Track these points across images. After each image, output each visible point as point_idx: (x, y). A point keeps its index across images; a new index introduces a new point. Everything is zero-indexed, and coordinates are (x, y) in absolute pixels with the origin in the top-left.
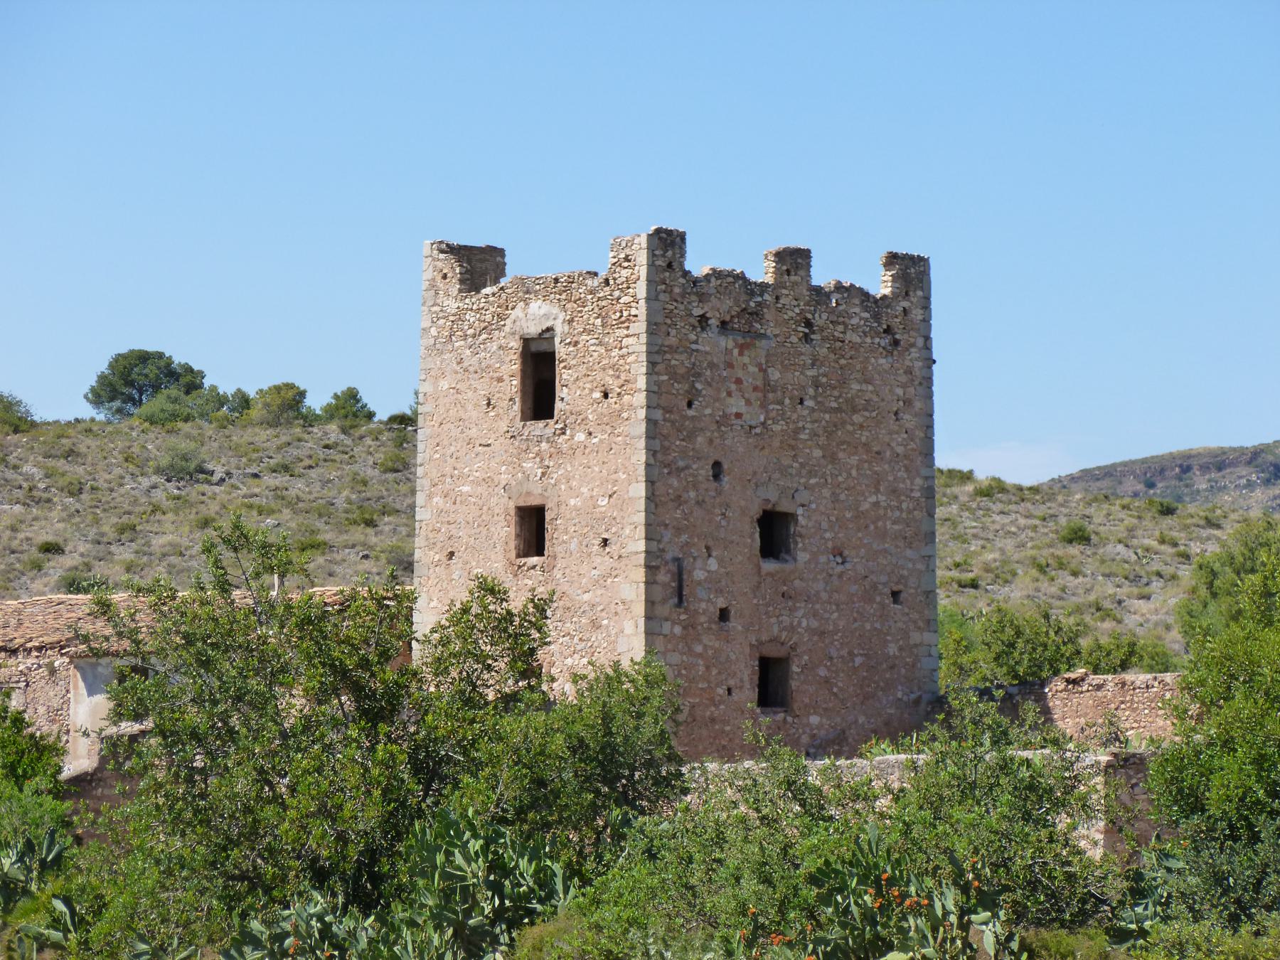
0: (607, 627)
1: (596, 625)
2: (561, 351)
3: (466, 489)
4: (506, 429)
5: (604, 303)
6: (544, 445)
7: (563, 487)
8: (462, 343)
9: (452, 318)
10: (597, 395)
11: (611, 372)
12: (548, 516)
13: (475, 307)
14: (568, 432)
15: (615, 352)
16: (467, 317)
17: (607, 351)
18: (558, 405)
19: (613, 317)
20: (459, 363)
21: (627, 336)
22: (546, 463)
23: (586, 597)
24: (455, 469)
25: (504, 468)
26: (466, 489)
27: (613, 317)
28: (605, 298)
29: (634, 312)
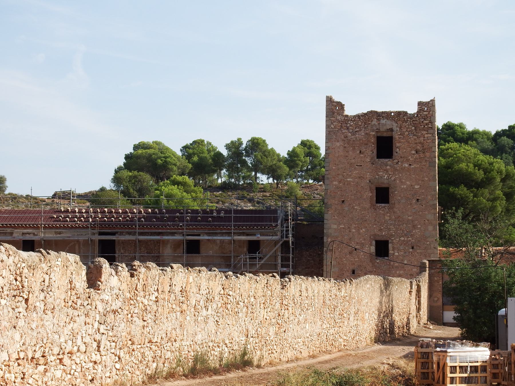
0: (420, 228)
1: (414, 227)
2: (396, 136)
3: (349, 180)
4: (369, 161)
5: (415, 122)
6: (388, 167)
7: (398, 181)
8: (347, 131)
9: (341, 122)
10: (414, 152)
11: (420, 145)
12: (390, 190)
13: (353, 119)
14: (399, 163)
15: (422, 139)
16: (349, 122)
17: (418, 138)
21: (427, 134)
22: (390, 173)
23: (410, 218)
24: (344, 173)
25: (368, 174)
26: (349, 180)
27: (420, 127)
29: (429, 126)
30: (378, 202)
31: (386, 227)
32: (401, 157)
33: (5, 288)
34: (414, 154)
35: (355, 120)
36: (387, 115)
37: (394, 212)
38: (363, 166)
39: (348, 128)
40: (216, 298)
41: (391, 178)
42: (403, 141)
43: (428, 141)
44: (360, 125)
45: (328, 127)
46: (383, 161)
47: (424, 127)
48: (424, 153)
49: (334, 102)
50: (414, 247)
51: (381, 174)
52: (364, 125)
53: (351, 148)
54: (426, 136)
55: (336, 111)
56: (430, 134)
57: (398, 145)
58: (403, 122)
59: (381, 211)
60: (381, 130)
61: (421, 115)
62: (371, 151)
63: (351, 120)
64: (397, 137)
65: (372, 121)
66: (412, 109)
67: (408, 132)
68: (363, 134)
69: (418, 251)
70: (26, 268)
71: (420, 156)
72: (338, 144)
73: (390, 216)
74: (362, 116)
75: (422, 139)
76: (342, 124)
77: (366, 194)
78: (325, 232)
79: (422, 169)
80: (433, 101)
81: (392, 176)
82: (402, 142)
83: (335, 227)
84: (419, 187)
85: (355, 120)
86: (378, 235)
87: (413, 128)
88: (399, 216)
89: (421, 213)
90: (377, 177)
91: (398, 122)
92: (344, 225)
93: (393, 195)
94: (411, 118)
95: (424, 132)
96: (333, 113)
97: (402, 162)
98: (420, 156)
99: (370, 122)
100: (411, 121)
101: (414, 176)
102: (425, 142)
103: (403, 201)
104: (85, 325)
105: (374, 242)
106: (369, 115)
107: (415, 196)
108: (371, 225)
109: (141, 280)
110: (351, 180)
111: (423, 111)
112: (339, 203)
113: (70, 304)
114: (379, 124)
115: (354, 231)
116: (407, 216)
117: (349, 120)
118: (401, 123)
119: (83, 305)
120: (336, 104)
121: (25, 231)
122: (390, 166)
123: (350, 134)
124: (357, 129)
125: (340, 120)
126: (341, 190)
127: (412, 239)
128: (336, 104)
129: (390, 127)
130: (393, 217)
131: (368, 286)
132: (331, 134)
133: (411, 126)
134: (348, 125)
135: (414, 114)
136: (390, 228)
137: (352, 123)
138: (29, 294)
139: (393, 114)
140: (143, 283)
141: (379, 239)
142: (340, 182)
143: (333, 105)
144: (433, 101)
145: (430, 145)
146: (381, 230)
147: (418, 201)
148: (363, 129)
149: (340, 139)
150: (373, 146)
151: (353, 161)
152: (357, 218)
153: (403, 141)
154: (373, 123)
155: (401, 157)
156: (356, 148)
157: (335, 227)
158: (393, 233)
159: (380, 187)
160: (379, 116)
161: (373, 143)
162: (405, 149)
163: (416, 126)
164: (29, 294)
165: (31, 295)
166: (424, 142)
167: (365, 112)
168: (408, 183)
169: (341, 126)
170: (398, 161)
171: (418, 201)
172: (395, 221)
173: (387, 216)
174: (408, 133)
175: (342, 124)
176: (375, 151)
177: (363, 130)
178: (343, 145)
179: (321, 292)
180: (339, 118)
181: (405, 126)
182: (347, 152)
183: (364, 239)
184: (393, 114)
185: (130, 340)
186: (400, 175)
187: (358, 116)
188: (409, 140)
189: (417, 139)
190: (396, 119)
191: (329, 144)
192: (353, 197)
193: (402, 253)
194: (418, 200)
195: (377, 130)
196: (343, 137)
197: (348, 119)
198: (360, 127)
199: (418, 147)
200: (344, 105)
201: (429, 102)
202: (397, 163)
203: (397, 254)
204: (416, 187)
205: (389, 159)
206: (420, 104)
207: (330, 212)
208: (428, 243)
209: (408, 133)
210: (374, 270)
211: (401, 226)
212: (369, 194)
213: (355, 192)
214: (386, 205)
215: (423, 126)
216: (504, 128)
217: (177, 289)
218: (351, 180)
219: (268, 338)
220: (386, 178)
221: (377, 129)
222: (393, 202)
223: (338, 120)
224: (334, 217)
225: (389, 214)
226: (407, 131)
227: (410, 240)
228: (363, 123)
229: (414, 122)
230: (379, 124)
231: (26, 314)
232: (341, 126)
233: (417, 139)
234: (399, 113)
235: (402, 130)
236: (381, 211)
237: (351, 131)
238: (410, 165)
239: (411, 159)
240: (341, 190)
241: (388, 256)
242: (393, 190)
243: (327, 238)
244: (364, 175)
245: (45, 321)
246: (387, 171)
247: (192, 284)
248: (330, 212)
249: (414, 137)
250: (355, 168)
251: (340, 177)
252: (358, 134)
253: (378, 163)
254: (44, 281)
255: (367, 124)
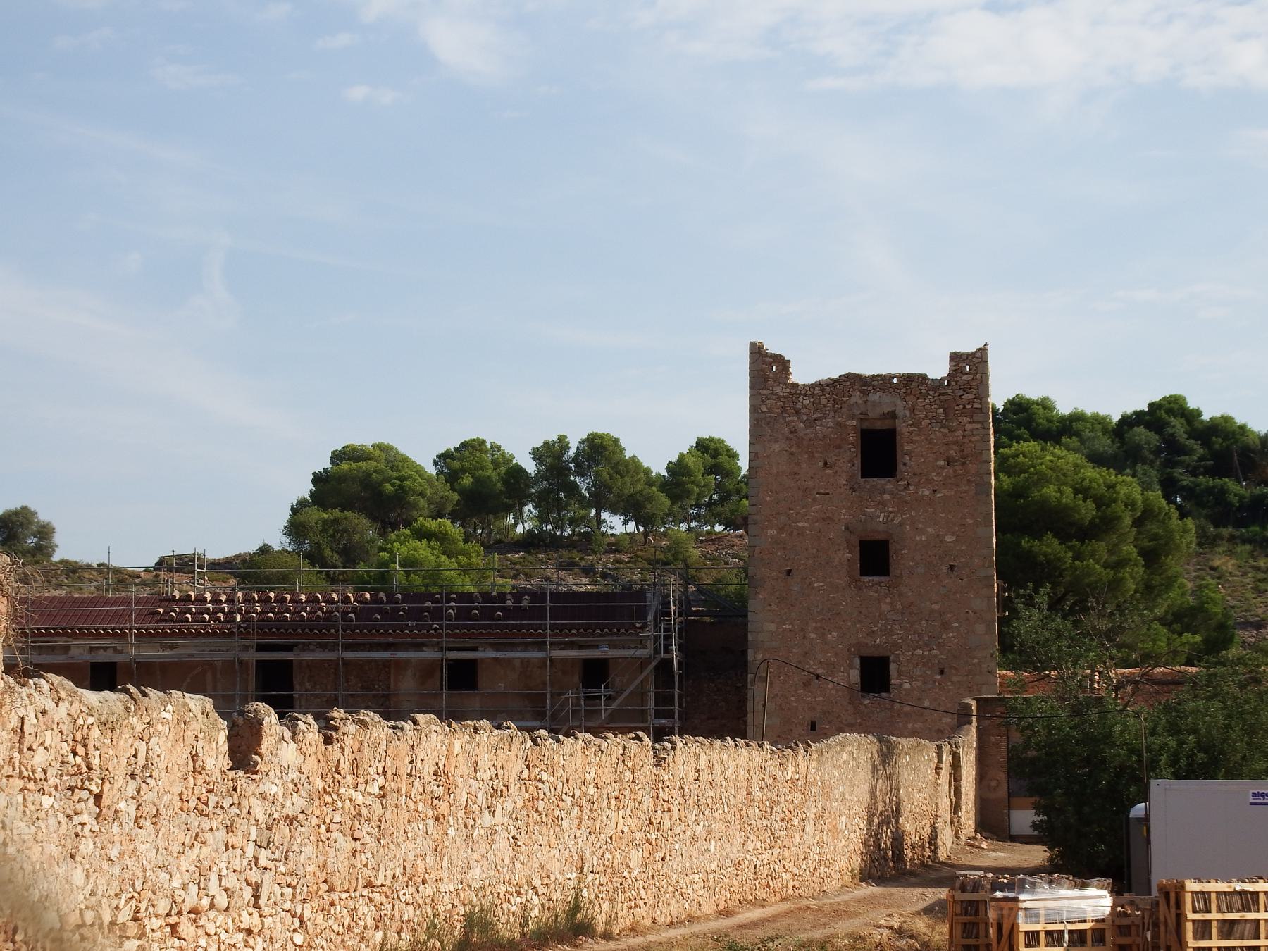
1: (945, 626)
2: (903, 429)
3: (800, 524)
4: (844, 482)
5: (945, 397)
6: (887, 497)
7: (908, 527)
8: (796, 419)
9: (782, 399)
10: (942, 463)
11: (955, 447)
12: (891, 547)
13: (809, 393)
14: (911, 488)
15: (960, 433)
16: (801, 399)
18: (900, 467)
19: (956, 408)
20: (791, 432)
21: (970, 422)
22: (890, 509)
23: (936, 607)
24: (790, 509)
26: (800, 524)
27: (956, 408)
28: (947, 394)
29: (976, 406)
30: (865, 572)
31: (883, 628)
32: (915, 474)
33: (51, 772)
34: (942, 468)
35: (813, 395)
36: (881, 382)
37: (901, 595)
38: (831, 495)
39: (797, 413)
40: (513, 788)
41: (892, 520)
42: (917, 438)
43: (973, 439)
44: (825, 406)
45: (753, 409)
46: (874, 483)
47: (964, 407)
48: (964, 464)
49: (766, 355)
50: (945, 670)
51: (872, 512)
52: (834, 406)
53: (806, 456)
54: (968, 427)
55: (771, 375)
56: (978, 422)
57: (907, 447)
58: (918, 398)
59: (871, 594)
60: (871, 415)
61: (956, 382)
62: (849, 462)
63: (805, 395)
64: (905, 430)
65: (850, 396)
66: (938, 370)
67: (930, 419)
68: (831, 424)
69: (954, 679)
70: (95, 725)
71: (955, 471)
72: (777, 447)
73: (891, 603)
74: (828, 385)
75: (960, 433)
76: (784, 402)
77: (840, 555)
78: (750, 638)
79: (960, 500)
80: (982, 351)
81: (894, 517)
82: (916, 441)
83: (772, 627)
84: (953, 538)
85: (813, 395)
86: (867, 644)
87: (941, 410)
88: (912, 603)
89: (958, 596)
90: (862, 518)
91: (907, 398)
92: (791, 624)
93: (897, 557)
94: (935, 389)
95: (965, 420)
96: (766, 379)
97: (917, 485)
98: (955, 471)
99: (845, 399)
100: (936, 394)
101: (943, 515)
102: (966, 440)
103: (920, 570)
104: (227, 849)
105: (857, 662)
106: (844, 383)
107: (947, 559)
108: (849, 624)
109: (347, 751)
110: (806, 524)
111: (961, 372)
112: (781, 575)
113: (192, 804)
114: (865, 402)
115: (813, 635)
116: (928, 603)
117: (800, 395)
118: (914, 399)
119: (222, 808)
120: (771, 360)
121: (96, 643)
122: (891, 493)
123: (802, 425)
124: (818, 415)
125: (781, 394)
126: (784, 548)
127: (941, 654)
128: (771, 360)
129: (889, 409)
130: (899, 606)
131: (845, 757)
132: (761, 426)
133: (936, 406)
134: (799, 406)
135: (943, 379)
136: (891, 630)
137: (808, 402)
138: (102, 784)
139: (895, 381)
140: (352, 757)
141: (867, 652)
142: (781, 530)
143: (764, 362)
144: (982, 351)
145: (977, 448)
146: (871, 634)
147: (952, 570)
148: (832, 414)
149: (780, 437)
150: (852, 450)
151: (810, 483)
152: (820, 607)
153: (917, 438)
154: (853, 400)
155: (915, 474)
156: (816, 455)
157: (772, 627)
158: (900, 641)
159: (869, 539)
160: (865, 384)
161: (852, 444)
162: (922, 456)
163: (946, 406)
164: (102, 784)
165: (107, 786)
166: (964, 440)
167: (835, 376)
168: (929, 530)
169: (784, 408)
170: (909, 484)
171: (952, 570)
172: (903, 613)
173: (886, 603)
174: (928, 421)
175: (784, 402)
176: (858, 462)
177: (830, 416)
178: (787, 449)
179: (742, 772)
180: (778, 389)
181: (924, 406)
182: (798, 464)
183: (836, 655)
184: (895, 381)
185: (325, 881)
186: (913, 514)
187: (820, 386)
188: (932, 436)
189: (949, 435)
190: (904, 390)
191: (758, 448)
192: (810, 562)
193: (919, 684)
194: (952, 567)
195: (861, 416)
196: (786, 431)
197: (798, 392)
198: (824, 409)
199: (951, 452)
200: (789, 361)
201: (974, 353)
202: (906, 487)
203: (907, 686)
204: (949, 539)
205: (887, 479)
206: (955, 357)
207: (761, 597)
208: (976, 661)
209: (928, 421)
210: (859, 721)
211: (917, 626)
212: (846, 556)
213: (815, 551)
214: (883, 579)
215: (961, 407)
216: (1139, 409)
217: (426, 769)
218: (806, 524)
219: (626, 874)
220: (881, 520)
221: (861, 414)
222: (899, 572)
223: (776, 394)
224: (769, 608)
225: (888, 600)
226: (926, 416)
227: (936, 656)
228: (831, 401)
229: (942, 397)
230: (865, 402)
231: (96, 828)
232: (784, 408)
233: (949, 435)
234: (908, 379)
235: (915, 415)
236: (871, 594)
237: (805, 418)
238: (934, 491)
239: (935, 479)
240: (784, 548)
241: (887, 690)
242: (898, 547)
243: (755, 653)
244: (833, 515)
245: (138, 843)
246: (884, 504)
247: (460, 757)
248: (761, 597)
249: (942, 430)
250: (814, 500)
251: (783, 519)
252: (821, 425)
253: (865, 488)
254: (135, 756)
255: (839, 402)
